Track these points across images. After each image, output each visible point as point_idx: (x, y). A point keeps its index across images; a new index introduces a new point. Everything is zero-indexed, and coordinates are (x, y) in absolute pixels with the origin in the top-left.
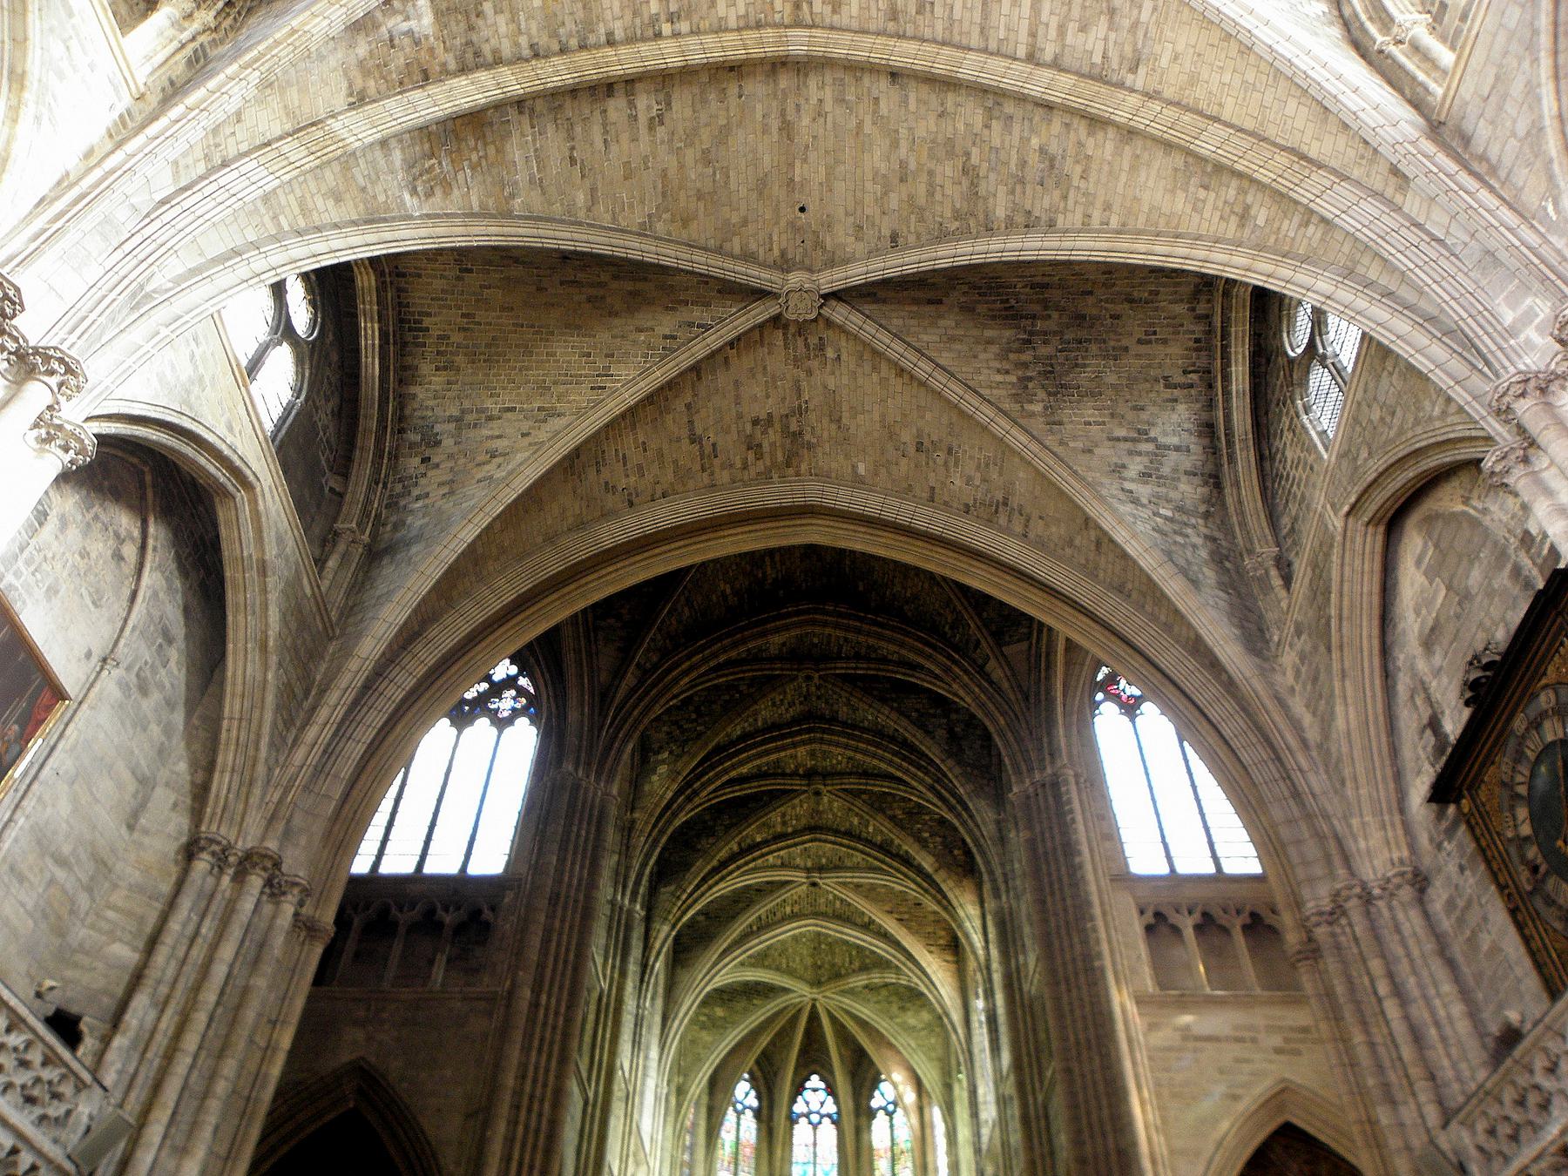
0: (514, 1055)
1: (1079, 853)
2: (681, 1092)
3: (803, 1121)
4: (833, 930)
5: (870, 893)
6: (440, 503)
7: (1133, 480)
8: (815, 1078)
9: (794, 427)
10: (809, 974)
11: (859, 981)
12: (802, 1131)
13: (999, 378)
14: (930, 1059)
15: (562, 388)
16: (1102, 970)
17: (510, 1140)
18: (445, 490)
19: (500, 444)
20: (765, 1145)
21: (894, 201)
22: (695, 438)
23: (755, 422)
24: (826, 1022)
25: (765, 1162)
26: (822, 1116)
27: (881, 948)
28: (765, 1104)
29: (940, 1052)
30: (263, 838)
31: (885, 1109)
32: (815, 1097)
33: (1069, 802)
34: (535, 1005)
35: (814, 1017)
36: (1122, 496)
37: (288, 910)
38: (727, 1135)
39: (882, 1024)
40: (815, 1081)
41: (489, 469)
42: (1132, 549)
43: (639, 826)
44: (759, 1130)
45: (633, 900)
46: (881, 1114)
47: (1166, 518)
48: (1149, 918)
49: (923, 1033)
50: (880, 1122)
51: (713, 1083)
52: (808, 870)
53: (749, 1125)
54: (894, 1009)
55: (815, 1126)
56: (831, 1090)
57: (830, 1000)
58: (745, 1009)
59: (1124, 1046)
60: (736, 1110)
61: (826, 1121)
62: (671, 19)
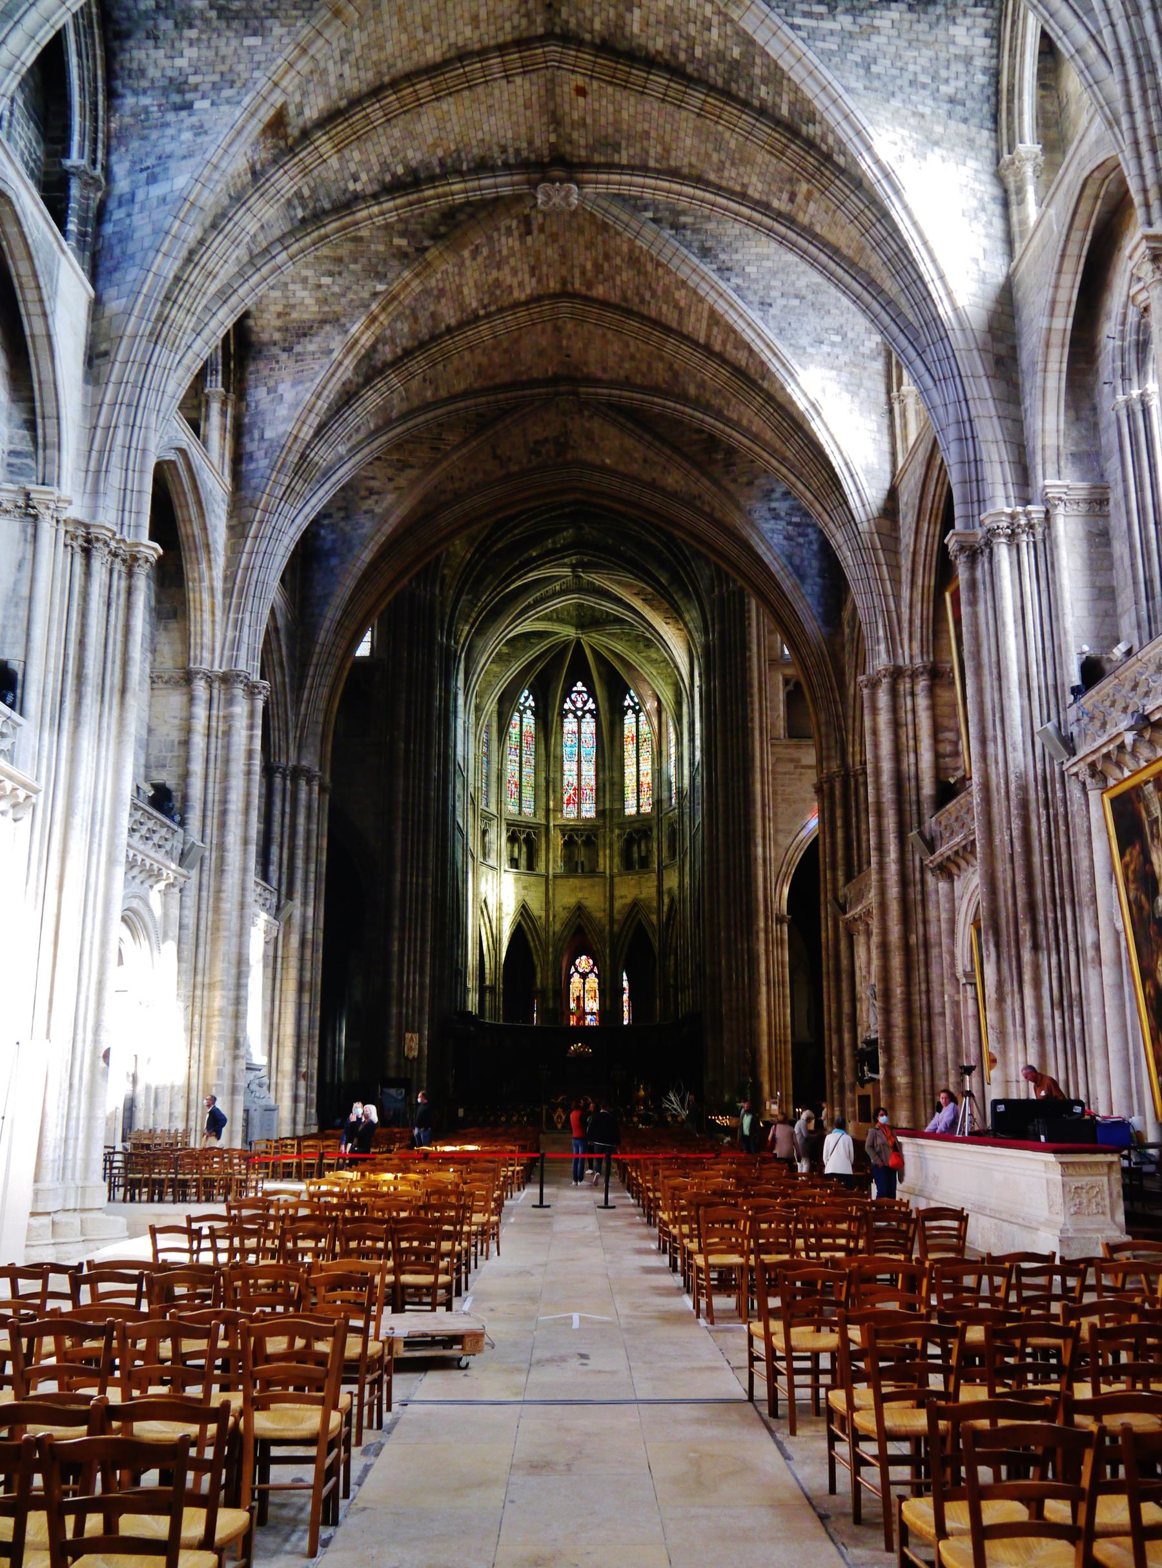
0: (401, 782)
1: (750, 650)
2: (478, 709)
3: (571, 716)
4: (590, 601)
5: (619, 583)
6: (342, 524)
7: (777, 500)
8: (579, 684)
9: (562, 440)
10: (574, 621)
11: (616, 629)
12: (570, 724)
13: (696, 437)
15: (410, 446)
16: (753, 729)
17: (405, 830)
18: (342, 514)
19: (375, 484)
20: (541, 735)
21: (627, 365)
22: (495, 457)
23: (536, 442)
24: (588, 651)
26: (585, 712)
27: (628, 616)
30: (299, 759)
31: (633, 708)
32: (579, 696)
33: (749, 611)
34: (407, 751)
35: (578, 642)
36: (768, 515)
37: (316, 788)
38: (514, 731)
39: (632, 657)
40: (580, 686)
41: (369, 503)
42: (768, 558)
43: (448, 580)
45: (449, 638)
46: (630, 712)
47: (797, 525)
48: (791, 687)
50: (629, 719)
51: (501, 701)
52: (573, 567)
53: (529, 720)
54: (641, 646)
55: (579, 720)
56: (591, 693)
57: (593, 640)
58: (525, 647)
59: (758, 776)
60: (519, 711)
61: (588, 716)
62: (484, 307)
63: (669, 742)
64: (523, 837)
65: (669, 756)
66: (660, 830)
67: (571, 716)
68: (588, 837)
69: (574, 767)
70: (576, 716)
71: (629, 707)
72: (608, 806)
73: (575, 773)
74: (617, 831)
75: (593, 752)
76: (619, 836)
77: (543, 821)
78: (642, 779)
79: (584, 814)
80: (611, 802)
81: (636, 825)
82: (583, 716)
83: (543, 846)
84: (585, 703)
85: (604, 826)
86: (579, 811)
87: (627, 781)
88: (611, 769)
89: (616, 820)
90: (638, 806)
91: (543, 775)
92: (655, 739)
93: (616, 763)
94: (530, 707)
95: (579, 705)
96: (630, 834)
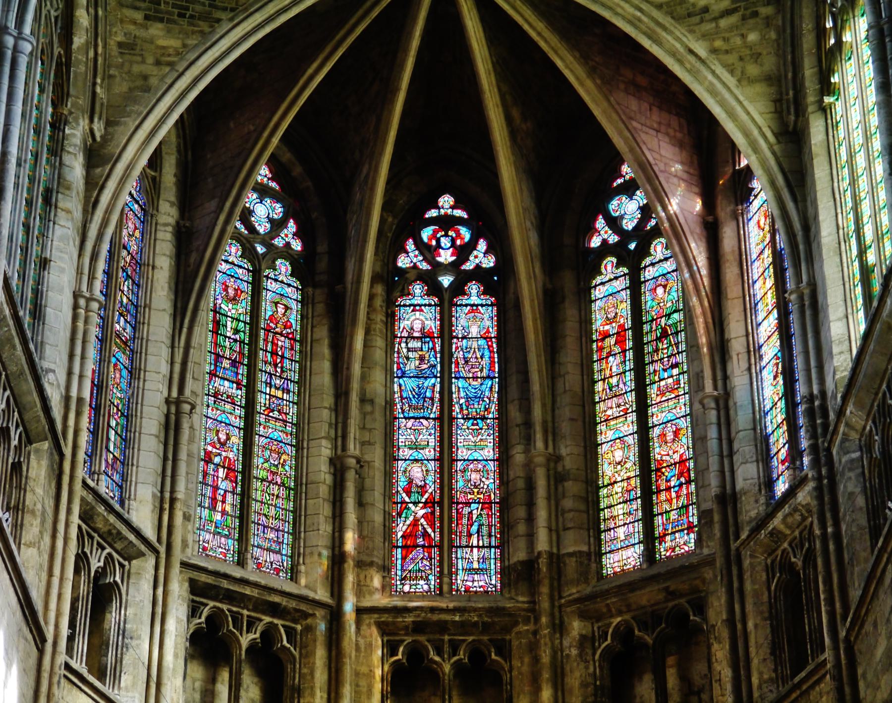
3: (418, 289)
8: (446, 201)
14: (744, 79)
20: (322, 333)
25: (324, 368)
28: (322, 248)
29: (769, 63)
31: (619, 251)
44: (303, 302)
46: (610, 260)
49: (724, 23)
60: (248, 253)
61: (474, 288)
63: (750, 308)
64: (245, 640)
65: (754, 351)
66: (735, 594)
67: (418, 289)
68: (477, 655)
69: (429, 436)
70: (434, 289)
71: (606, 249)
72: (543, 543)
73: (429, 453)
74: (577, 627)
75: (490, 389)
76: (586, 642)
77: (322, 594)
78: (658, 451)
79: (461, 579)
80: (556, 532)
81: (645, 597)
82: (458, 289)
83: (320, 676)
84: (463, 252)
85: (533, 612)
86: (446, 571)
87: (607, 470)
88: (552, 432)
89: (572, 591)
90: (650, 539)
91: (325, 450)
92: (699, 308)
93: (567, 411)
94: (286, 252)
95: (446, 257)
96: (624, 635)
